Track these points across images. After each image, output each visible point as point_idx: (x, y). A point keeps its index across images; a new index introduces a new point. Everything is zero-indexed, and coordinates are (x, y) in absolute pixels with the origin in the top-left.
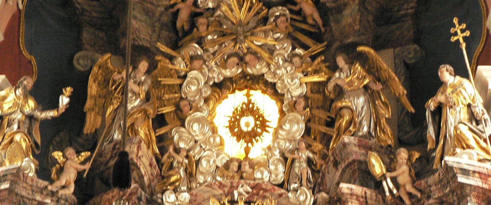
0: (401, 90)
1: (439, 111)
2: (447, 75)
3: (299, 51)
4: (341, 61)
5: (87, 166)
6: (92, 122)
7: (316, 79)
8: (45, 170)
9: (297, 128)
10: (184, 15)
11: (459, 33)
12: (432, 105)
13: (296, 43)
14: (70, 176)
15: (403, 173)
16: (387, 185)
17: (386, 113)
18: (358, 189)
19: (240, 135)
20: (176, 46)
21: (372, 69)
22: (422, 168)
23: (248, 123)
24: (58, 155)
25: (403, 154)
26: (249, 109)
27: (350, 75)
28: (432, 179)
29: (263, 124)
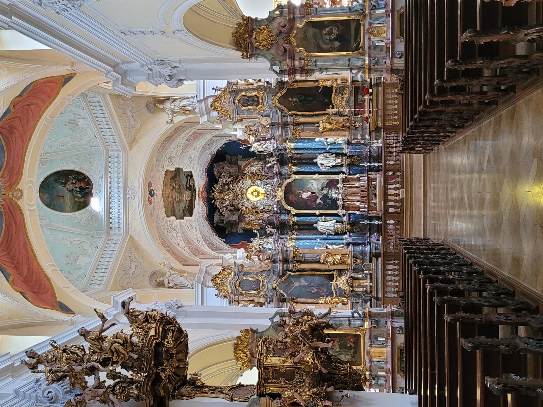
0: (252, 159)
1: (258, 151)
2: (252, 150)
3: (241, 182)
4: (245, 172)
5: (270, 226)
7: (248, 178)
9: (259, 182)
11: (243, 147)
12: (257, 153)
14: (272, 230)
16: (274, 163)
17: (256, 163)
18: (275, 169)
19: (258, 195)
20: (239, 210)
21: (246, 166)
22: (271, 155)
23: (255, 194)
24: (268, 232)
25: (268, 159)
26: (252, 193)
27: (249, 170)
28: (274, 153)
29: (256, 190)
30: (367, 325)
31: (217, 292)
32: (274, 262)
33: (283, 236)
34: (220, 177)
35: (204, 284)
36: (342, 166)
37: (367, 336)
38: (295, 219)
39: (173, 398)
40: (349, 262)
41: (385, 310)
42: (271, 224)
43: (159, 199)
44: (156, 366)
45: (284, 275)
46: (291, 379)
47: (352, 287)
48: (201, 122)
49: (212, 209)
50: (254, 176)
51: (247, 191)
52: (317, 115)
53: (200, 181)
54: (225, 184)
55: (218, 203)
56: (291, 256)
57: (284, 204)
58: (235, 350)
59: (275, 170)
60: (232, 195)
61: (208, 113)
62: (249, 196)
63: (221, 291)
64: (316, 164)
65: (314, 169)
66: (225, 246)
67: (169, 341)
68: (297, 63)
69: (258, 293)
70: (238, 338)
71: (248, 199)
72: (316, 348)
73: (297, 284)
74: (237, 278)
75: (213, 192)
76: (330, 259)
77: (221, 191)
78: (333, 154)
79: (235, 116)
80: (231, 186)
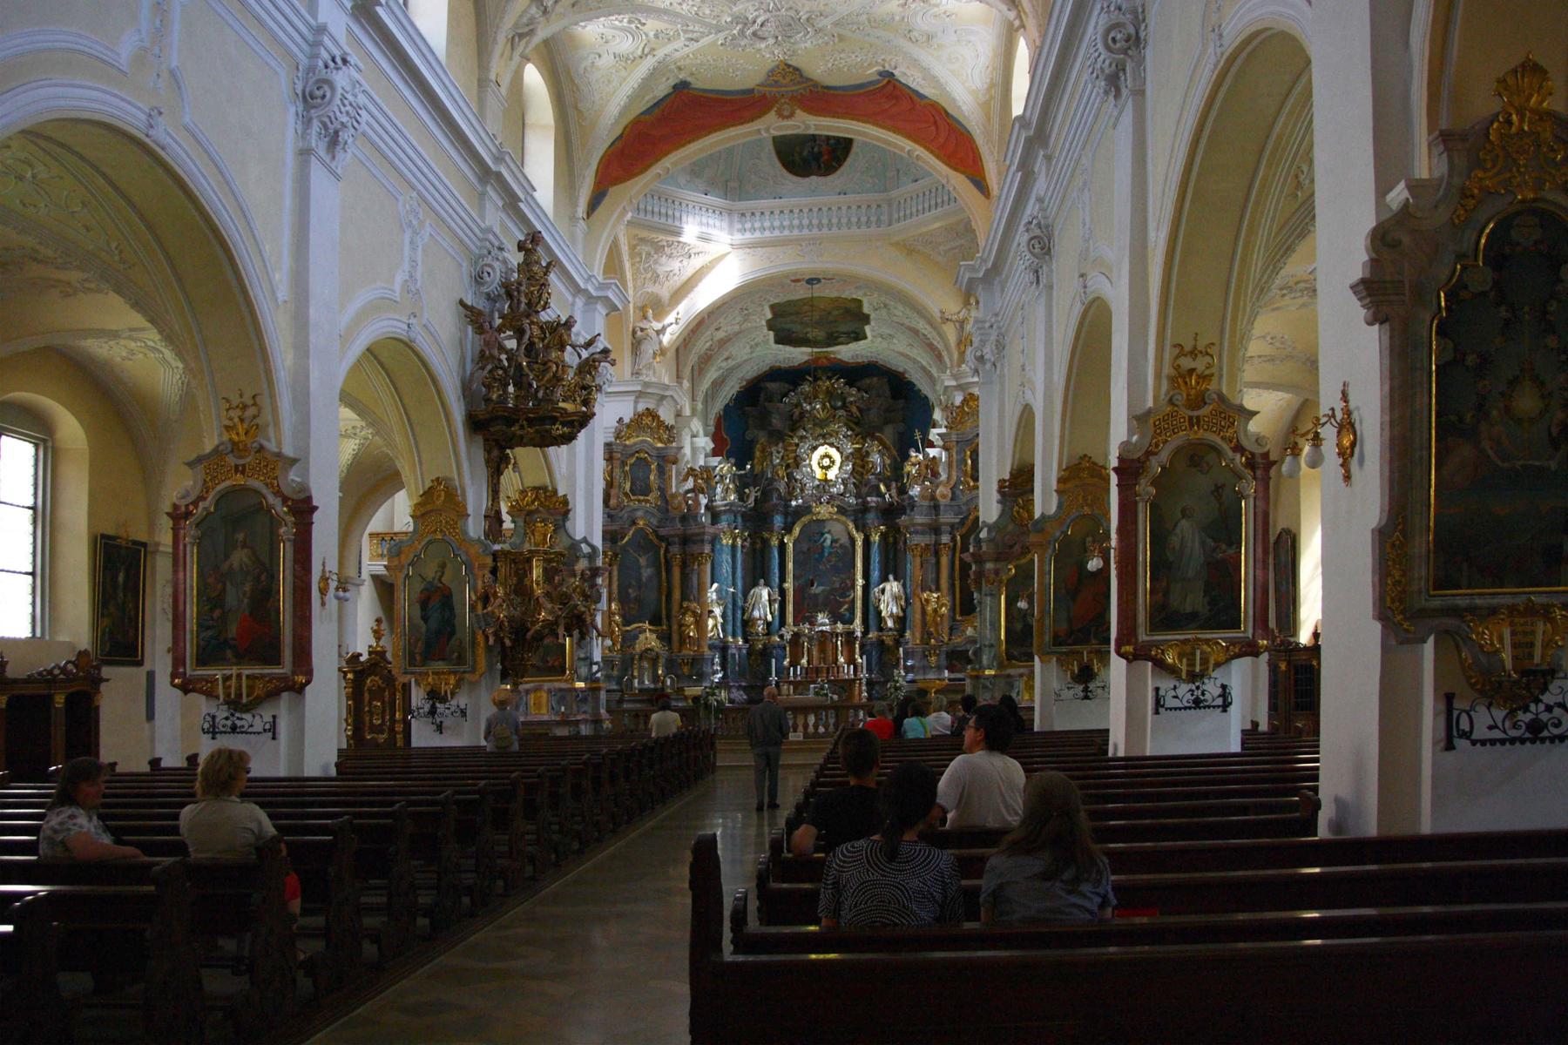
6: (758, 469)
8: (742, 497)
10: (797, 412)
11: (918, 436)
13: (849, 428)
14: (752, 500)
15: (894, 492)
20: (794, 430)
21: (881, 442)
23: (826, 462)
26: (827, 456)
30: (581, 685)
31: (627, 420)
32: (684, 519)
33: (739, 519)
34: (859, 390)
35: (640, 395)
36: (881, 629)
37: (563, 685)
38: (775, 542)
39: (486, 440)
40: (685, 652)
41: (603, 711)
42: (766, 495)
43: (802, 292)
44: (528, 419)
45: (661, 538)
46: (516, 592)
47: (641, 657)
48: (943, 377)
49: (791, 377)
50: (859, 460)
51: (831, 445)
52: (952, 586)
53: (847, 352)
54: (844, 400)
55: (806, 388)
56: (695, 549)
57: (805, 519)
58: (536, 489)
59: (872, 500)
60: (822, 415)
61: (959, 387)
62: (822, 450)
63: (628, 426)
64: (885, 579)
65: (875, 574)
66: (719, 406)
67: (558, 429)
68: (989, 566)
69: (626, 494)
70: (555, 492)
71: (815, 448)
72: (556, 623)
73: (643, 561)
74: (654, 453)
75: (830, 378)
76: (689, 619)
77: (830, 394)
78: (904, 610)
79: (954, 438)
80: (841, 412)
